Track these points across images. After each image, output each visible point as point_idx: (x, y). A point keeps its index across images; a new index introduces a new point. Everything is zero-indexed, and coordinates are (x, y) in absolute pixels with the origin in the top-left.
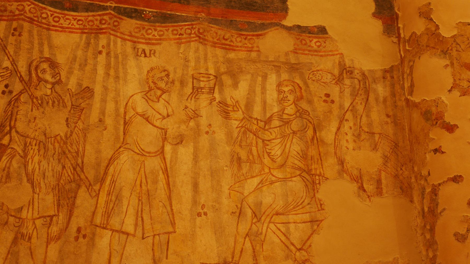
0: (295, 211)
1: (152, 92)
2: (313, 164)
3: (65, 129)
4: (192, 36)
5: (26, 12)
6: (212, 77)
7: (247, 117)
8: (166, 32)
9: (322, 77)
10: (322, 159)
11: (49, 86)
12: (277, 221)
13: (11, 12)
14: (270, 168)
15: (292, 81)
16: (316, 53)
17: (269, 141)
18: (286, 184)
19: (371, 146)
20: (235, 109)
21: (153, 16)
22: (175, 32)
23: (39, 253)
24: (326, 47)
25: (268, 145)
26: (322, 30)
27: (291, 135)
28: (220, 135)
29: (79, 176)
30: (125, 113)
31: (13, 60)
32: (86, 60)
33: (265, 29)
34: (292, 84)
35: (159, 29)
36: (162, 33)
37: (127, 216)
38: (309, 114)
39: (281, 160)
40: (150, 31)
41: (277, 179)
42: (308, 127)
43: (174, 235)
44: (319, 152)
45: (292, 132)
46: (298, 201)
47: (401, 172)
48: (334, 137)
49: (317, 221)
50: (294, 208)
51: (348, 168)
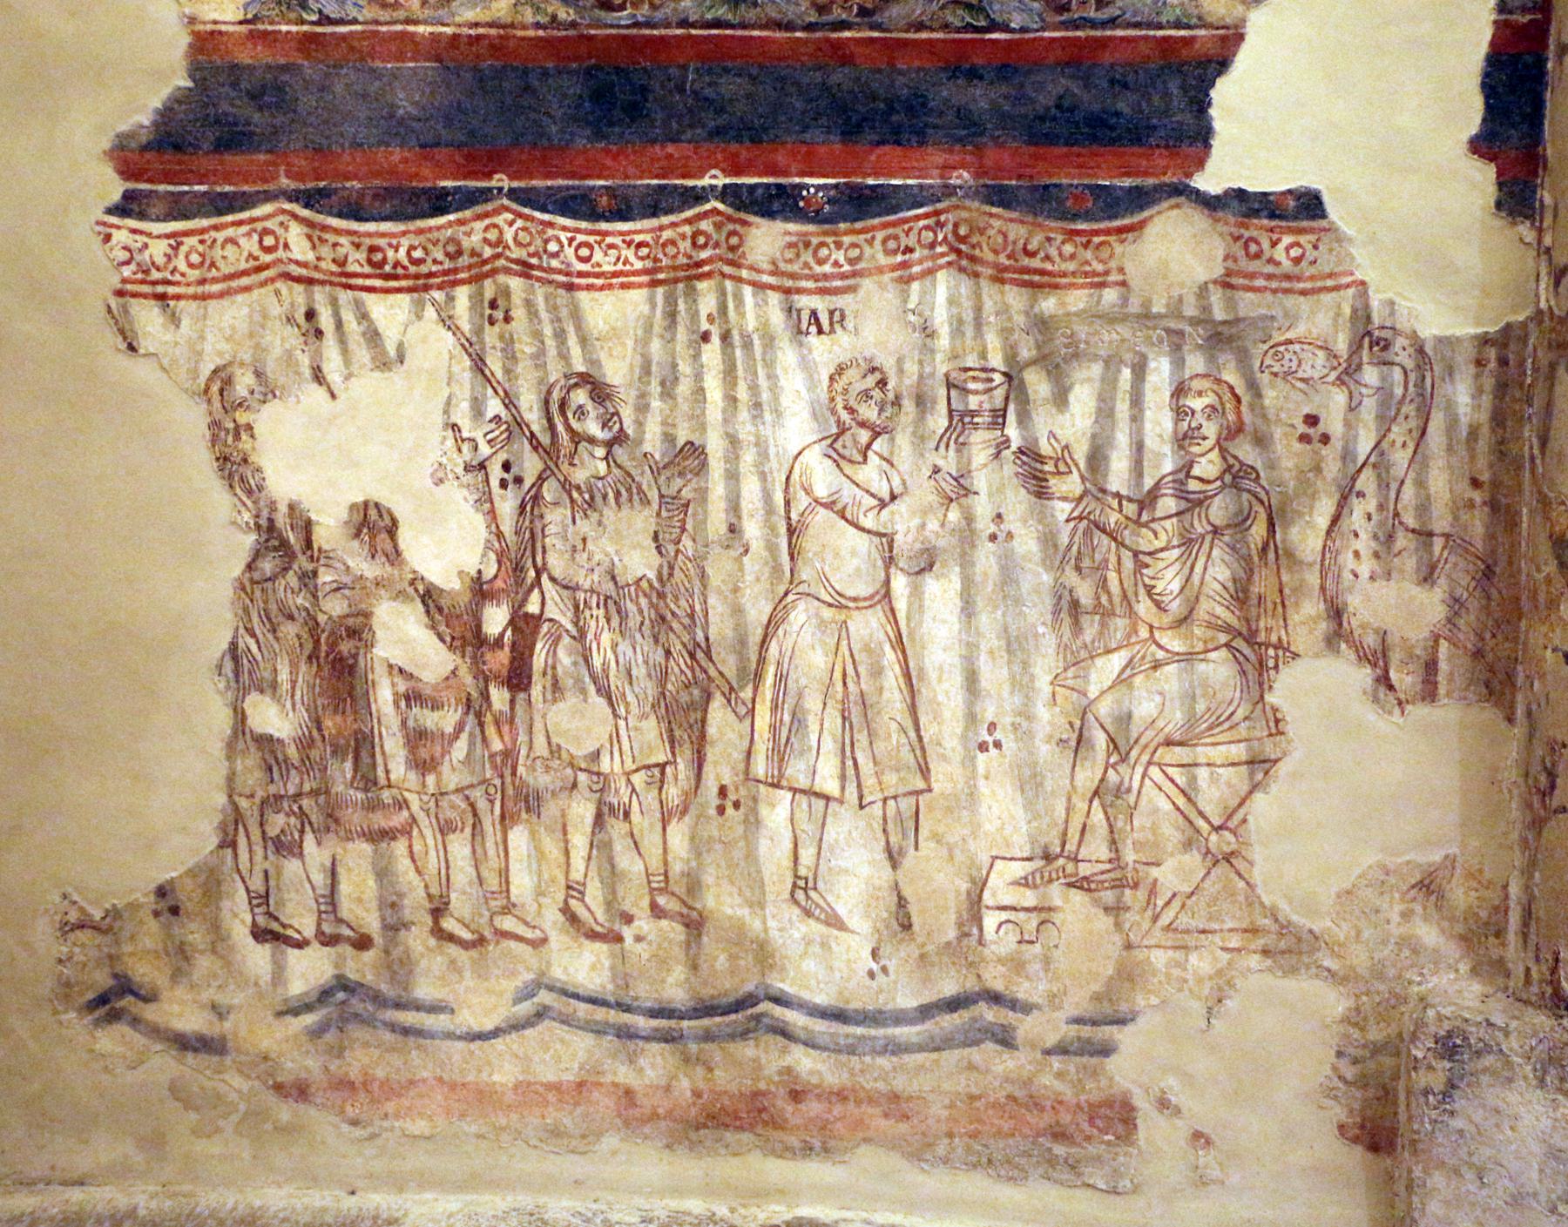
1: (847, 436)
3: (656, 560)
4: (939, 250)
5: (507, 247)
6: (998, 378)
7: (1093, 490)
8: (868, 251)
11: (600, 452)
12: (1167, 760)
13: (473, 253)
14: (1151, 627)
16: (1285, 285)
17: (1150, 554)
19: (1418, 570)
20: (1062, 468)
21: (829, 202)
22: (892, 245)
23: (652, 843)
25: (1147, 566)
26: (1309, 205)
27: (1208, 538)
28: (1027, 543)
29: (706, 672)
30: (788, 503)
31: (506, 392)
32: (674, 366)
33: (1142, 208)
34: (1215, 387)
35: (847, 240)
36: (855, 253)
37: (821, 758)
38: (1258, 476)
40: (824, 252)
43: (927, 796)
45: (1209, 528)
47: (1491, 643)
49: (1264, 761)
50: (1210, 728)
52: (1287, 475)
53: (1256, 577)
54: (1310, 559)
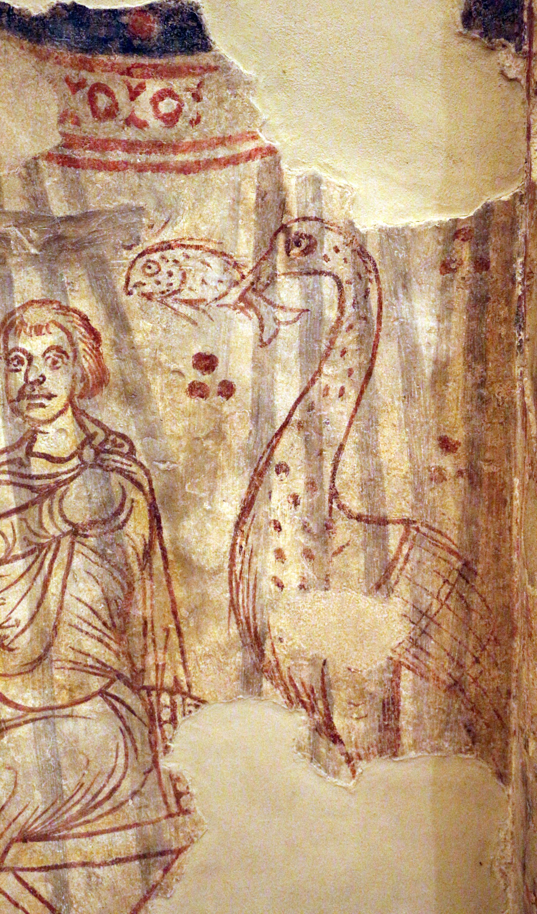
0: (88, 822)
2: (151, 649)
9: (184, 275)
10: (184, 629)
12: (24, 863)
15: (61, 307)
16: (156, 158)
18: (54, 730)
19: (367, 573)
24: (203, 119)
27: (66, 542)
34: (60, 319)
38: (132, 449)
39: (31, 640)
41: (21, 713)
42: (128, 504)
44: (173, 601)
46: (95, 789)
47: (474, 671)
48: (227, 541)
49: (162, 853)
50: (83, 813)
51: (281, 658)
52: (174, 445)
53: (138, 595)
54: (213, 564)
